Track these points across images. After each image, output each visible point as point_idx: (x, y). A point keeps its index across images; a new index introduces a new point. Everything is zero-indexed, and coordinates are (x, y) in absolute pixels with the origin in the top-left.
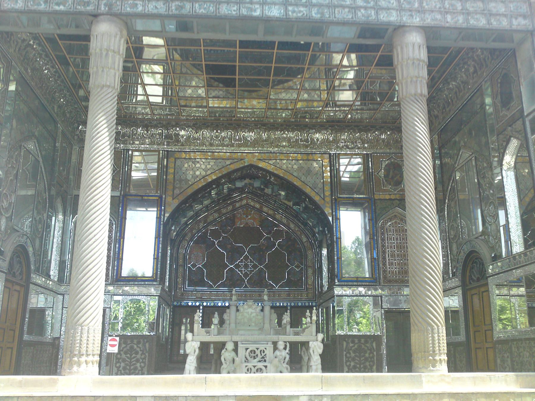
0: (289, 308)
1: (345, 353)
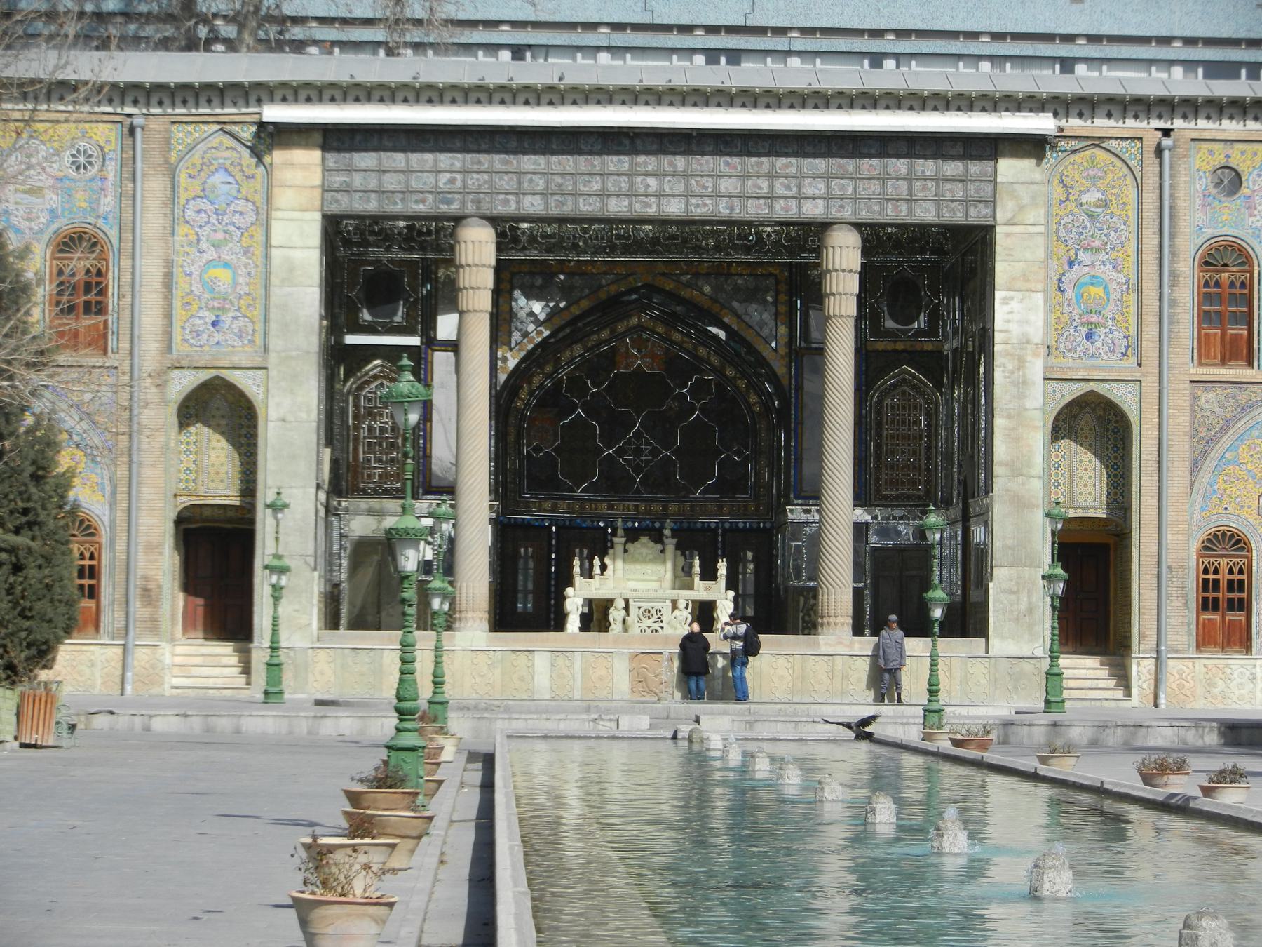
0: (720, 531)
1: (801, 615)
